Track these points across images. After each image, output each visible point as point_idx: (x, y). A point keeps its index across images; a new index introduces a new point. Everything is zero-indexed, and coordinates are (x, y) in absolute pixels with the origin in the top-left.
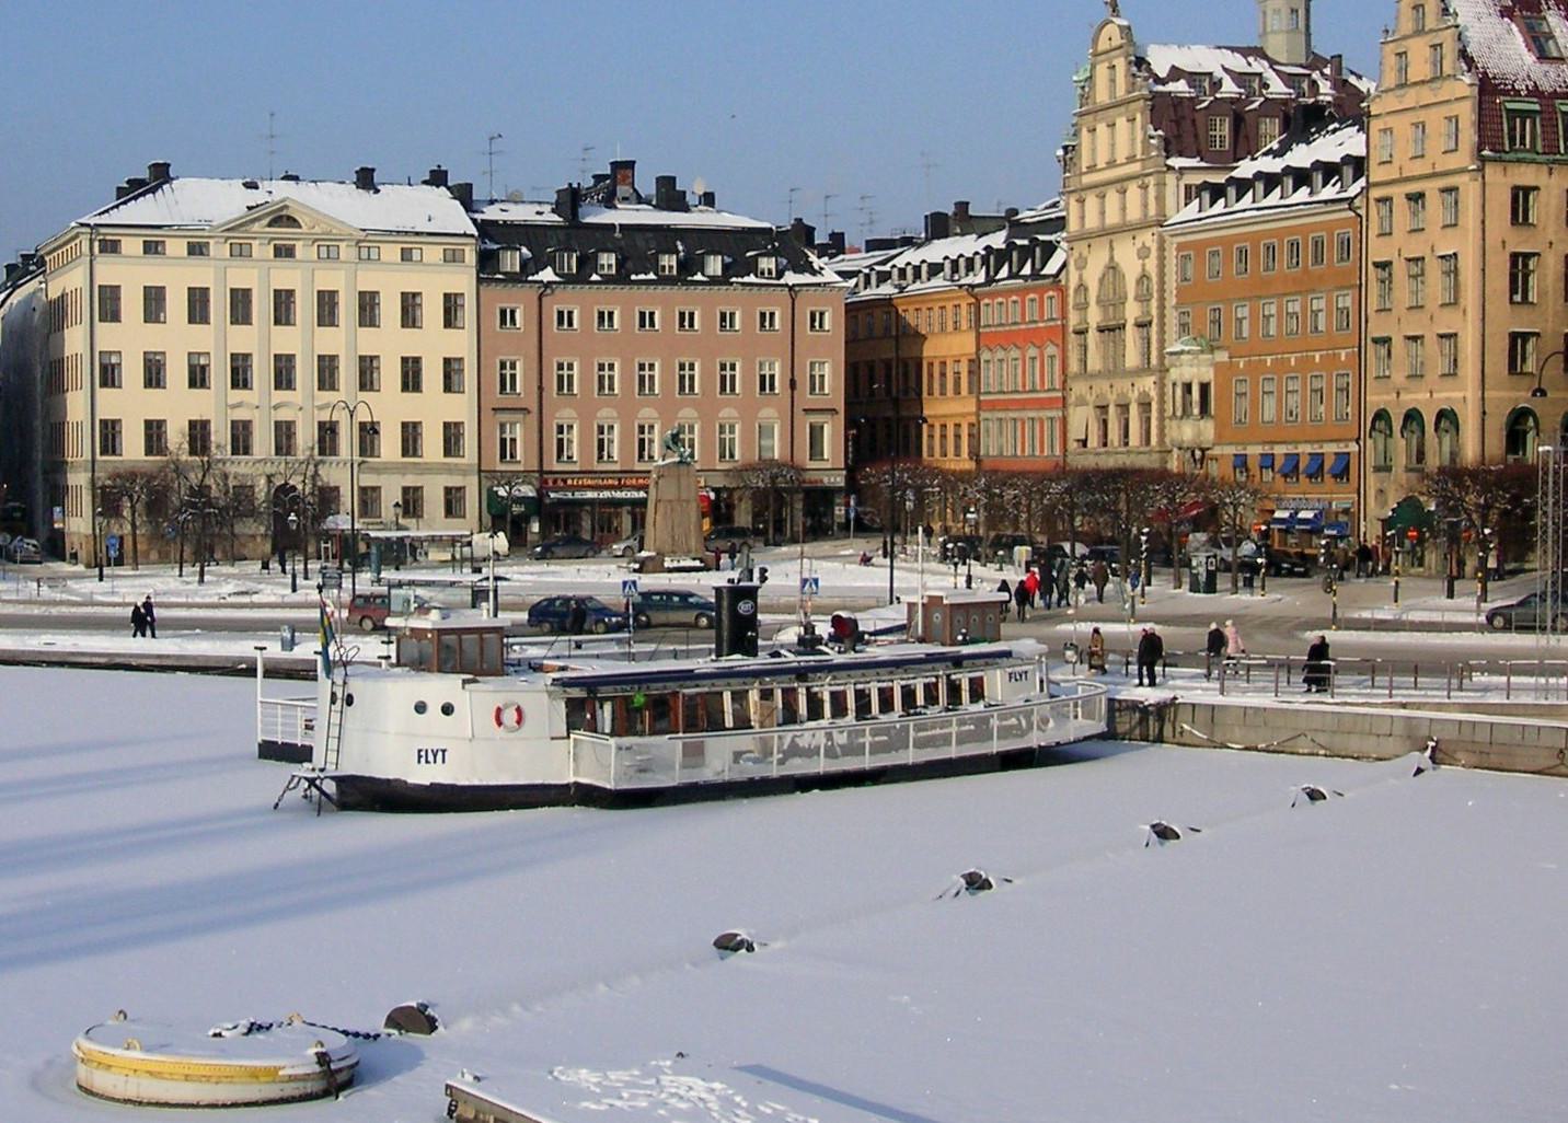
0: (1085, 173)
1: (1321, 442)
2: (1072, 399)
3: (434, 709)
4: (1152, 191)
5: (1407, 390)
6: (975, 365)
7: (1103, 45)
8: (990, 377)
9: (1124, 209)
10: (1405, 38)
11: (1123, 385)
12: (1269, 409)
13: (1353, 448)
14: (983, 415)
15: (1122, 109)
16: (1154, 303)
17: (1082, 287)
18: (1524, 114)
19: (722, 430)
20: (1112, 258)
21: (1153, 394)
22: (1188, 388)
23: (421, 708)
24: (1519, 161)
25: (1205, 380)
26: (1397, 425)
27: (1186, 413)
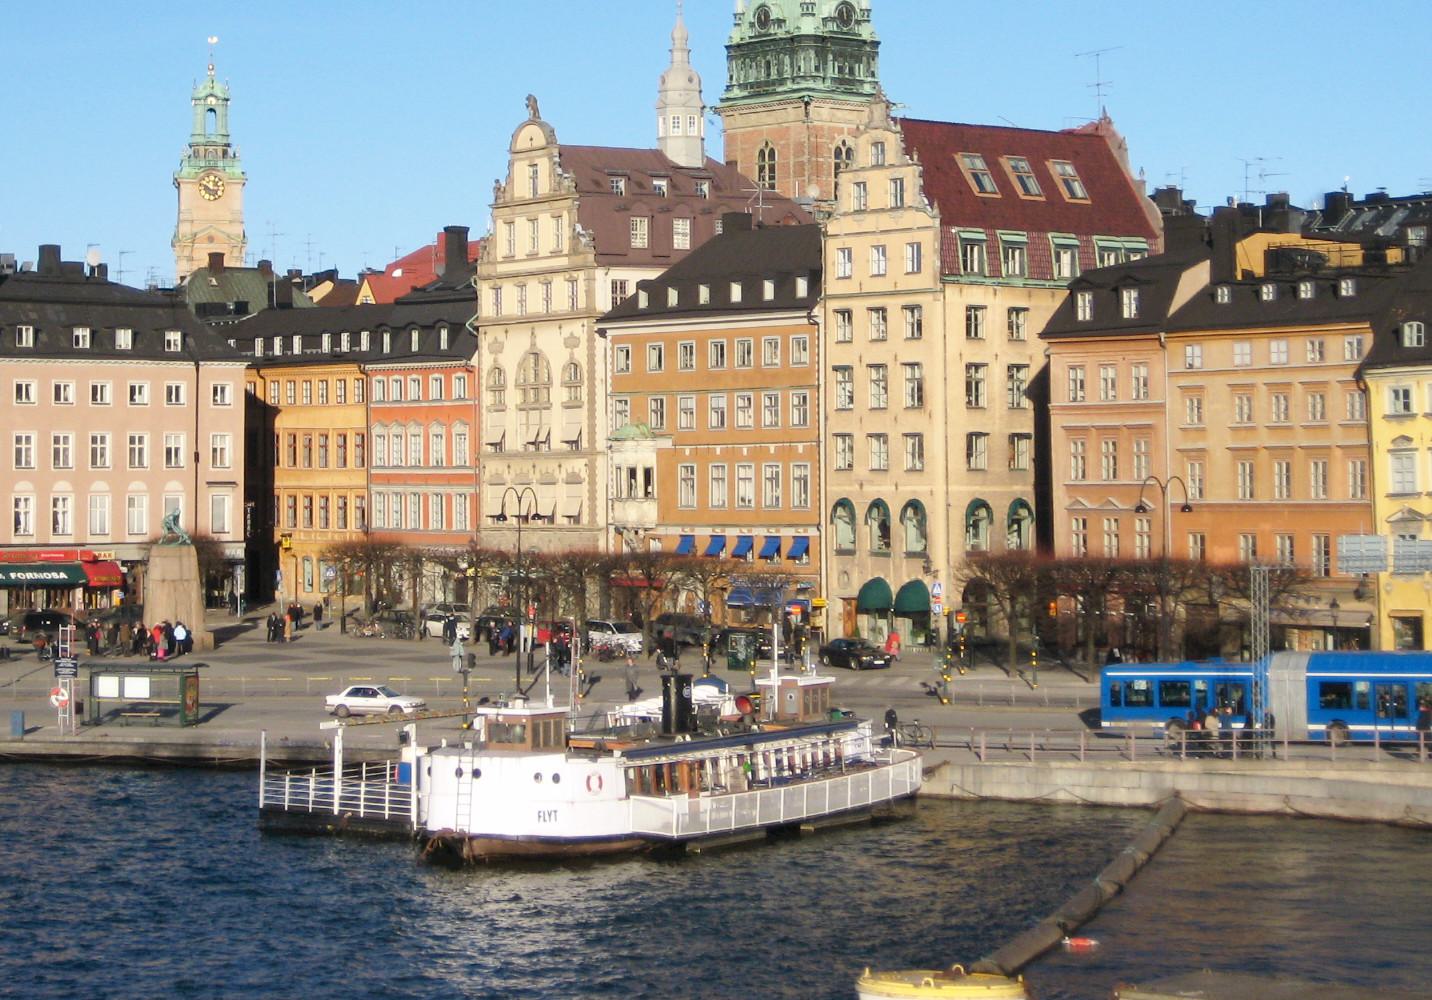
0: (501, 262)
1: (777, 526)
2: (486, 476)
3: (547, 777)
4: (581, 286)
5: (871, 482)
6: (364, 441)
7: (522, 143)
8: (378, 449)
9: (548, 300)
10: (863, 169)
12: (718, 494)
13: (812, 532)
14: (375, 489)
16: (584, 390)
18: (973, 243)
19: (55, 501)
20: (533, 345)
22: (633, 473)
23: (537, 777)
24: (972, 283)
25: (648, 466)
26: (860, 512)
27: (631, 497)
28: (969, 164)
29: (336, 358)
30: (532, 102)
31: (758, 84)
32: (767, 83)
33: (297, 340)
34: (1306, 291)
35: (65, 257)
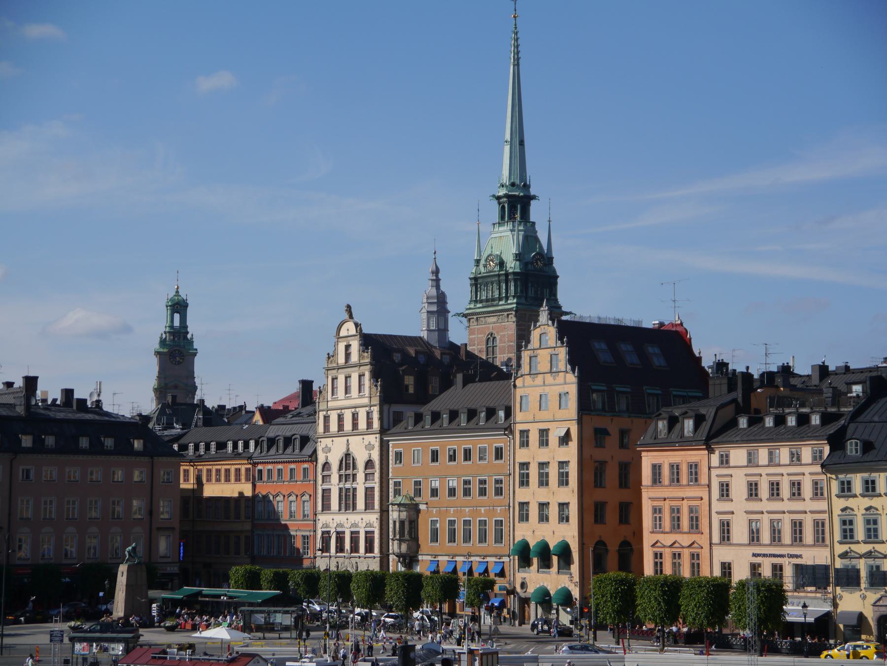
11: (353, 518)
15: (356, 369)
17: (326, 466)
21: (377, 525)
28: (600, 346)
29: (236, 455)
30: (349, 308)
31: (487, 300)
32: (493, 300)
33: (213, 445)
34: (791, 421)
35: (77, 395)
